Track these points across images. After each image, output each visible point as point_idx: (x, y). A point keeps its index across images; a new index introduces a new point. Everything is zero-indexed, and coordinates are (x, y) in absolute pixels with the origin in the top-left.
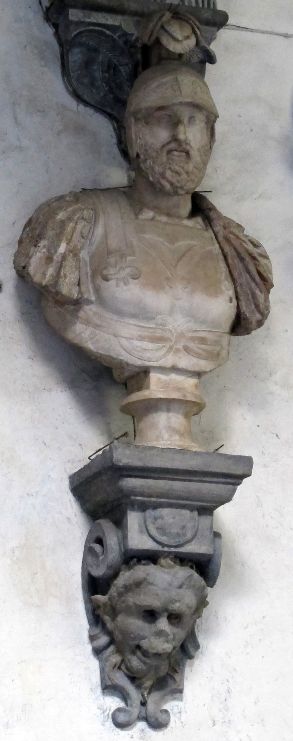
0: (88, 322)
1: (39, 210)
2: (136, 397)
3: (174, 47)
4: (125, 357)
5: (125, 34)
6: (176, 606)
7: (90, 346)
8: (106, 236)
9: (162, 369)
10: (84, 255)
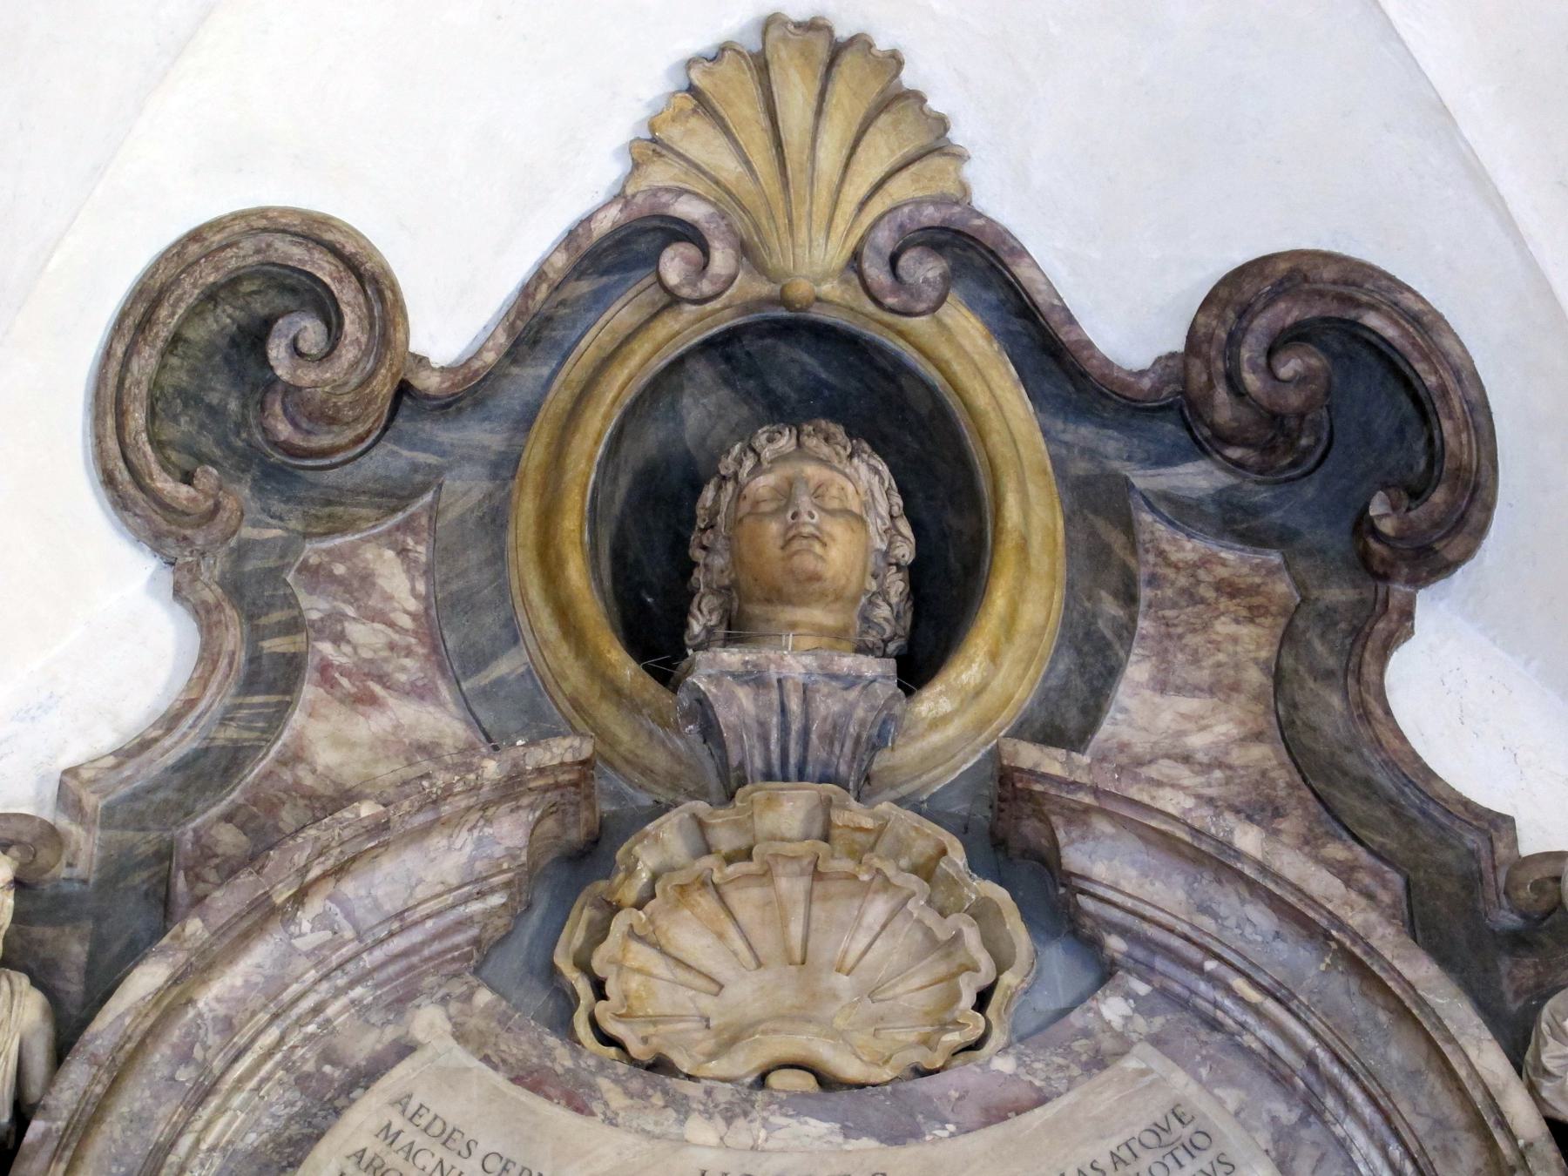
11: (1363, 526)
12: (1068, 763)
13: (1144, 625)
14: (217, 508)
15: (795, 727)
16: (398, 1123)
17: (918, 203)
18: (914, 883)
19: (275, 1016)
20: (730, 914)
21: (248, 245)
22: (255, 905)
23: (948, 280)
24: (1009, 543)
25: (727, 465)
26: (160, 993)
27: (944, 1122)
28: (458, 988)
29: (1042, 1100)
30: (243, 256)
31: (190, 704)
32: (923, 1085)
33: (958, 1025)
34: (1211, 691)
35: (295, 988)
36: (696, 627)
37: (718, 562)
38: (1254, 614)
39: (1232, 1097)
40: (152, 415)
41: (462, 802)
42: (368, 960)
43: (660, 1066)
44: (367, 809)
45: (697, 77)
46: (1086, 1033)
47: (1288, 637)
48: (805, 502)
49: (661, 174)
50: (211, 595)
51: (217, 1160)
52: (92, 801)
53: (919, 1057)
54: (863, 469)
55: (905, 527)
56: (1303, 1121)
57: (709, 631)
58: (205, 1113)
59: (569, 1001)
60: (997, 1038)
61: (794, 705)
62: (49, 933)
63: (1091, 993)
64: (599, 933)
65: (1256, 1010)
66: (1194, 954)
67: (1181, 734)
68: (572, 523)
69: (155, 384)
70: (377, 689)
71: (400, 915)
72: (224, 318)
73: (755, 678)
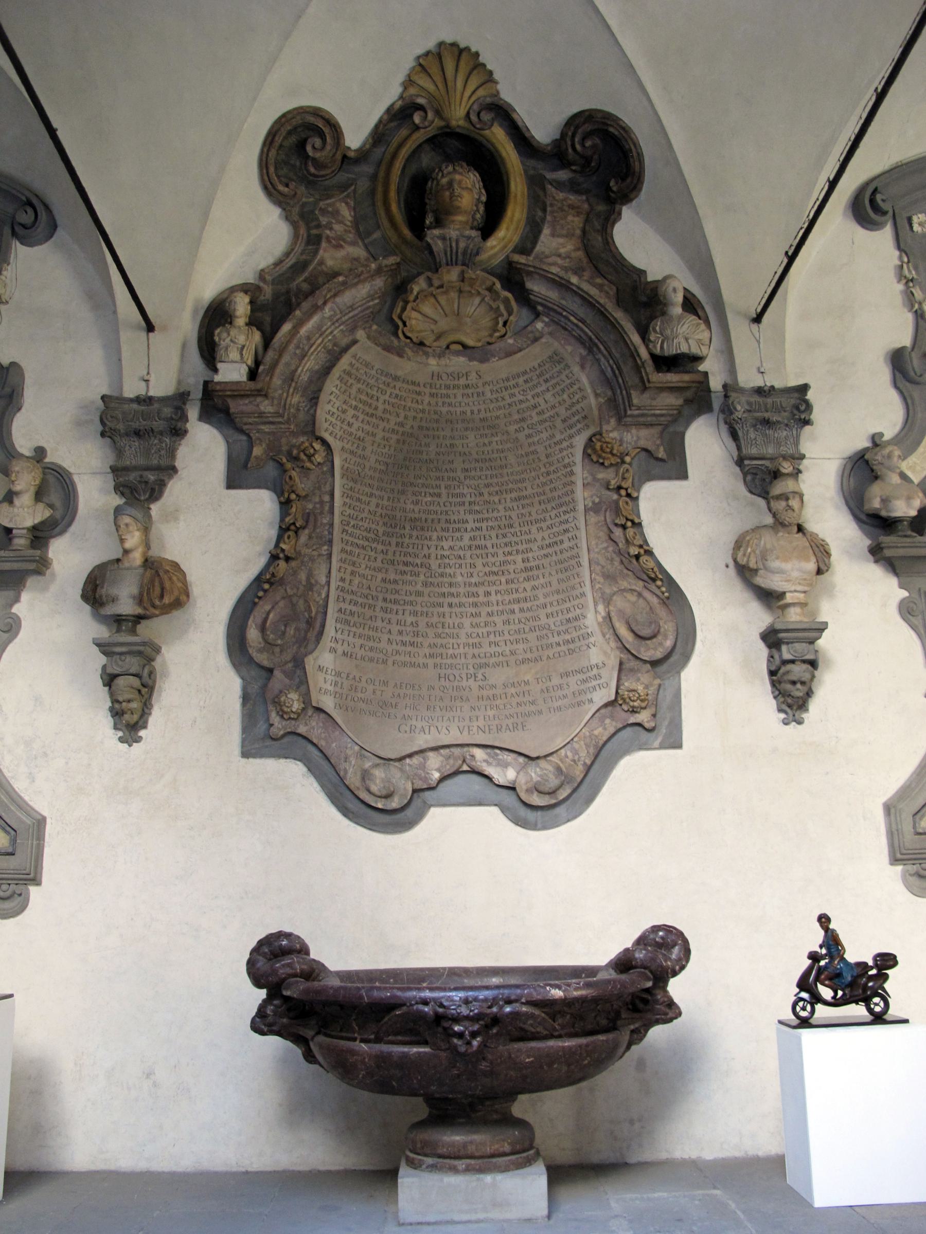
0: (761, 577)
1: (740, 536)
2: (781, 603)
3: (784, 471)
4: (777, 589)
5: (767, 467)
6: (803, 679)
7: (763, 585)
8: (765, 544)
9: (791, 592)
10: (758, 552)
11: (609, 189)
12: (527, 260)
13: (549, 218)
14: (296, 194)
15: (454, 251)
16: (354, 362)
17: (485, 97)
18: (487, 293)
19: (321, 335)
20: (438, 302)
21: (298, 118)
22: (313, 306)
23: (493, 120)
24: (512, 195)
25: (434, 175)
26: (290, 331)
27: (495, 357)
28: (368, 325)
29: (520, 350)
30: (298, 121)
31: (293, 250)
32: (489, 347)
33: (498, 331)
34: (567, 237)
35: (325, 327)
36: (427, 222)
37: (433, 203)
38: (578, 214)
39: (569, 348)
40: (276, 168)
41: (366, 275)
42: (344, 319)
43: (422, 344)
44: (341, 279)
45: (421, 60)
46: (532, 332)
47: (587, 221)
48: (456, 186)
49: (412, 91)
50: (296, 218)
51: (308, 374)
52: (268, 278)
53: (488, 339)
54: (472, 176)
55: (483, 191)
56: (588, 354)
57: (431, 223)
58: (304, 362)
59: (397, 327)
60: (509, 334)
61: (454, 245)
62: (260, 314)
63: (533, 322)
64: (404, 309)
65: (576, 325)
66: (560, 310)
67: (558, 249)
68: (393, 194)
69: (276, 159)
70: (342, 243)
71: (351, 307)
72: (293, 139)
73: (443, 238)
